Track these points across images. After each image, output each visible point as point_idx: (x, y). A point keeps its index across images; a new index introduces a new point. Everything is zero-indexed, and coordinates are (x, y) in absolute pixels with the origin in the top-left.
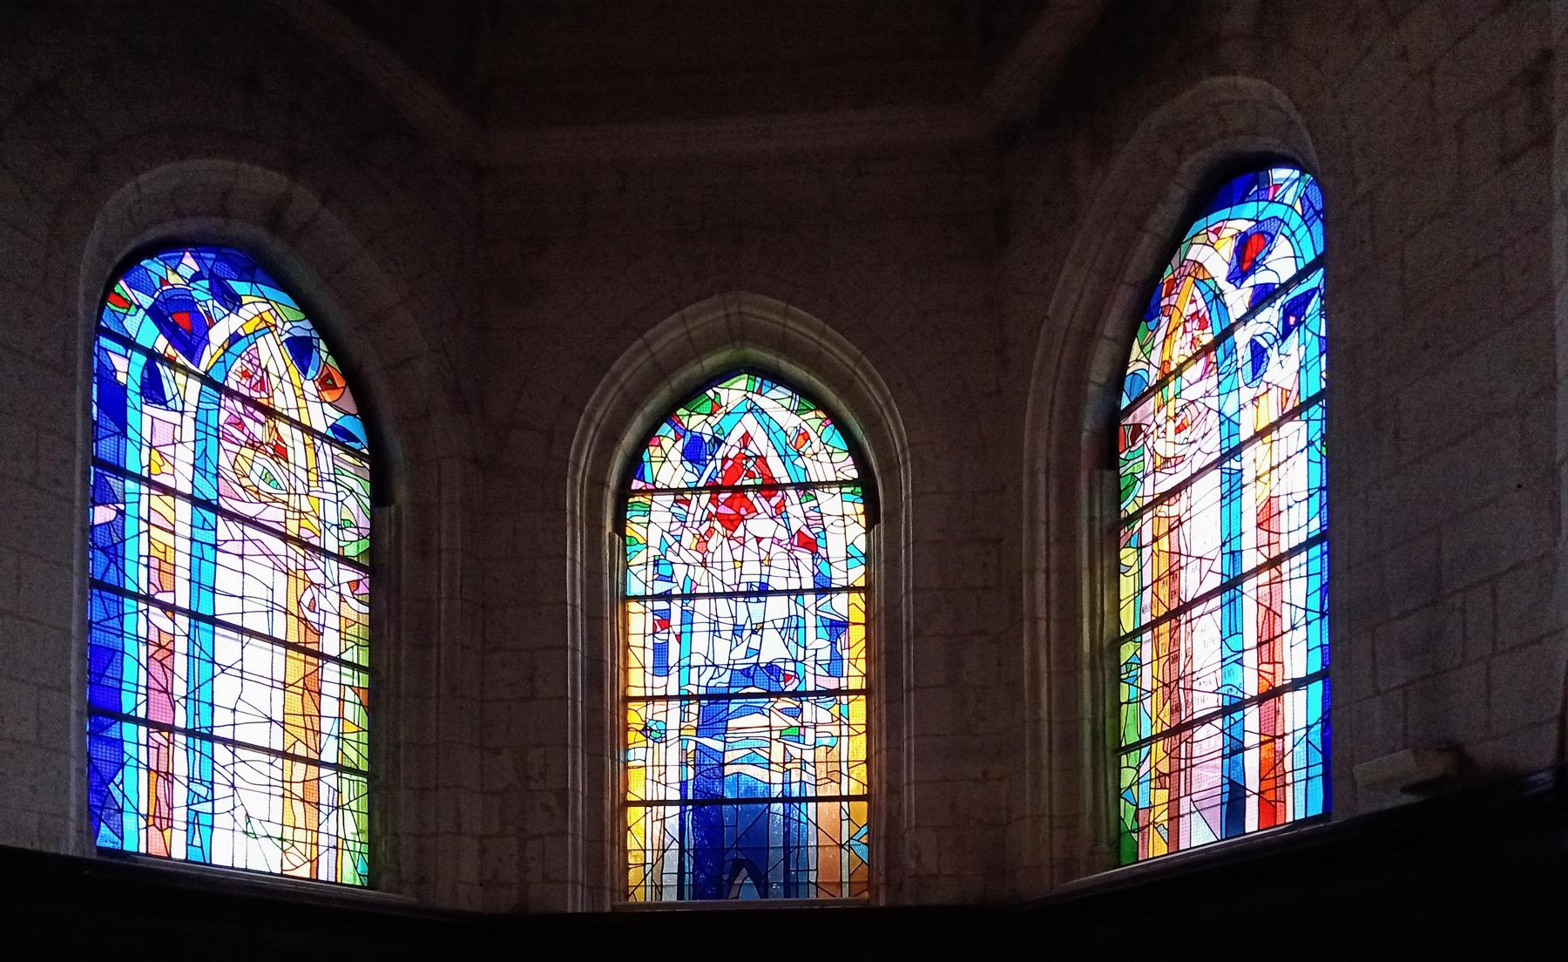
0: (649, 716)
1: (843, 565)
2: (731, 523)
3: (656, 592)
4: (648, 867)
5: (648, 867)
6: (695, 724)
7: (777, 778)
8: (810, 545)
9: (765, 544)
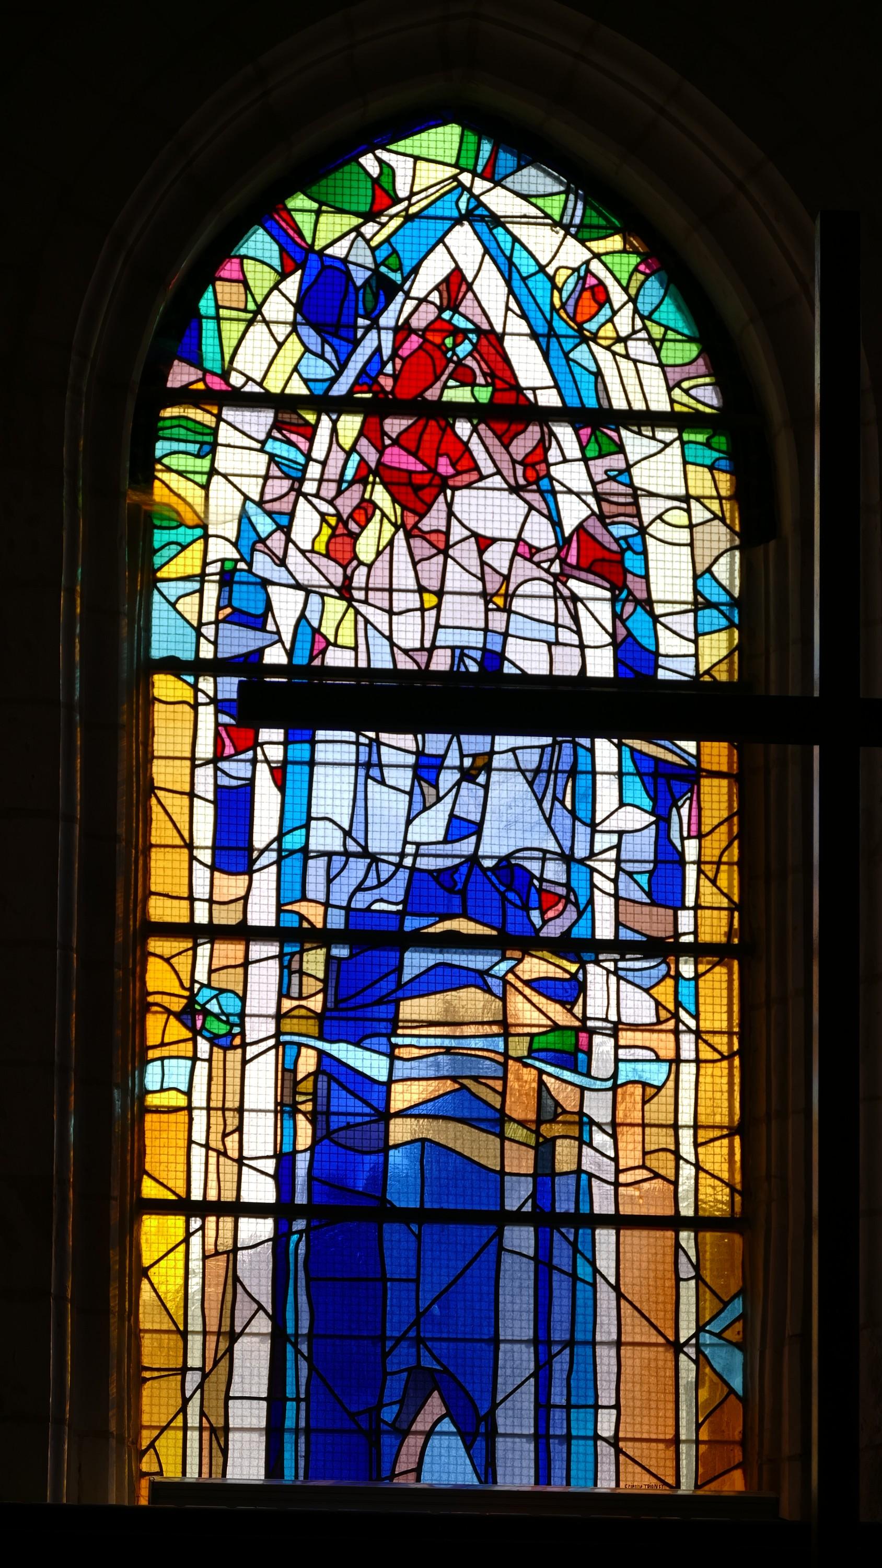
0: (201, 975)
1: (685, 624)
3: (226, 652)
4: (193, 1379)
5: (193, 1379)
6: (316, 1004)
9: (499, 556)
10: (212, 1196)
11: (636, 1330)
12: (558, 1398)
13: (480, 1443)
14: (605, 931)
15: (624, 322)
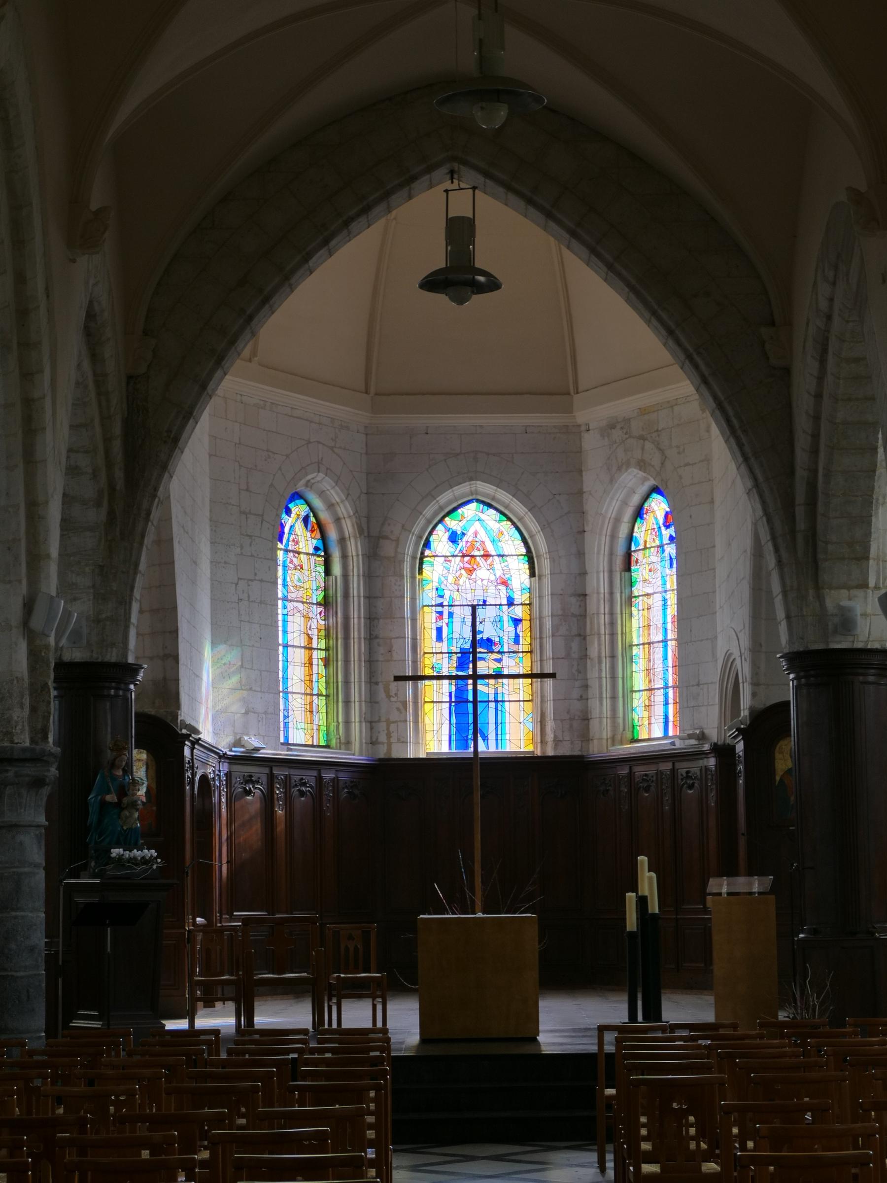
0: (434, 661)
1: (519, 593)
2: (470, 571)
3: (437, 603)
4: (435, 732)
5: (435, 732)
6: (455, 665)
7: (492, 691)
8: (505, 583)
9: (485, 582)
10: (478, 655)
11: (513, 720)
12: (499, 732)
13: (486, 741)
14: (506, 650)
15: (507, 537)
